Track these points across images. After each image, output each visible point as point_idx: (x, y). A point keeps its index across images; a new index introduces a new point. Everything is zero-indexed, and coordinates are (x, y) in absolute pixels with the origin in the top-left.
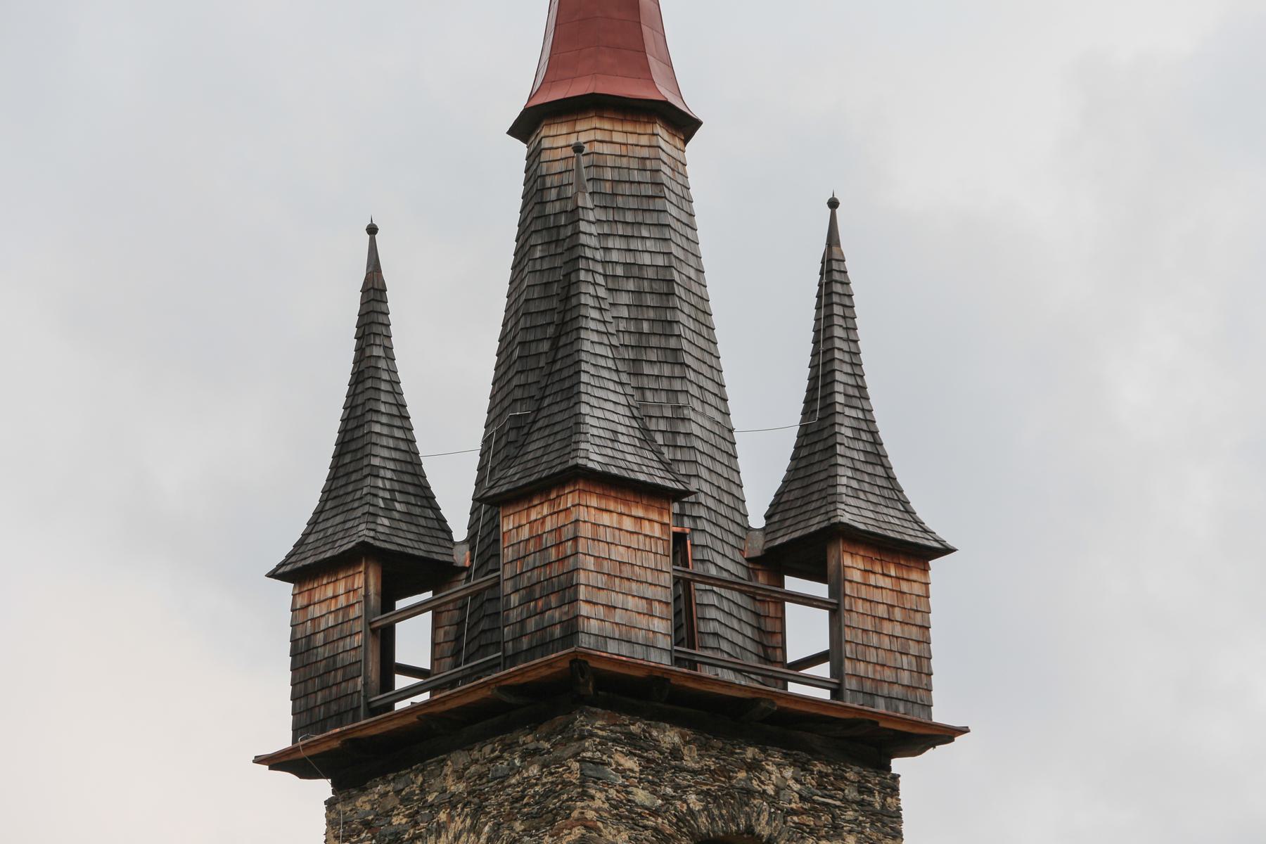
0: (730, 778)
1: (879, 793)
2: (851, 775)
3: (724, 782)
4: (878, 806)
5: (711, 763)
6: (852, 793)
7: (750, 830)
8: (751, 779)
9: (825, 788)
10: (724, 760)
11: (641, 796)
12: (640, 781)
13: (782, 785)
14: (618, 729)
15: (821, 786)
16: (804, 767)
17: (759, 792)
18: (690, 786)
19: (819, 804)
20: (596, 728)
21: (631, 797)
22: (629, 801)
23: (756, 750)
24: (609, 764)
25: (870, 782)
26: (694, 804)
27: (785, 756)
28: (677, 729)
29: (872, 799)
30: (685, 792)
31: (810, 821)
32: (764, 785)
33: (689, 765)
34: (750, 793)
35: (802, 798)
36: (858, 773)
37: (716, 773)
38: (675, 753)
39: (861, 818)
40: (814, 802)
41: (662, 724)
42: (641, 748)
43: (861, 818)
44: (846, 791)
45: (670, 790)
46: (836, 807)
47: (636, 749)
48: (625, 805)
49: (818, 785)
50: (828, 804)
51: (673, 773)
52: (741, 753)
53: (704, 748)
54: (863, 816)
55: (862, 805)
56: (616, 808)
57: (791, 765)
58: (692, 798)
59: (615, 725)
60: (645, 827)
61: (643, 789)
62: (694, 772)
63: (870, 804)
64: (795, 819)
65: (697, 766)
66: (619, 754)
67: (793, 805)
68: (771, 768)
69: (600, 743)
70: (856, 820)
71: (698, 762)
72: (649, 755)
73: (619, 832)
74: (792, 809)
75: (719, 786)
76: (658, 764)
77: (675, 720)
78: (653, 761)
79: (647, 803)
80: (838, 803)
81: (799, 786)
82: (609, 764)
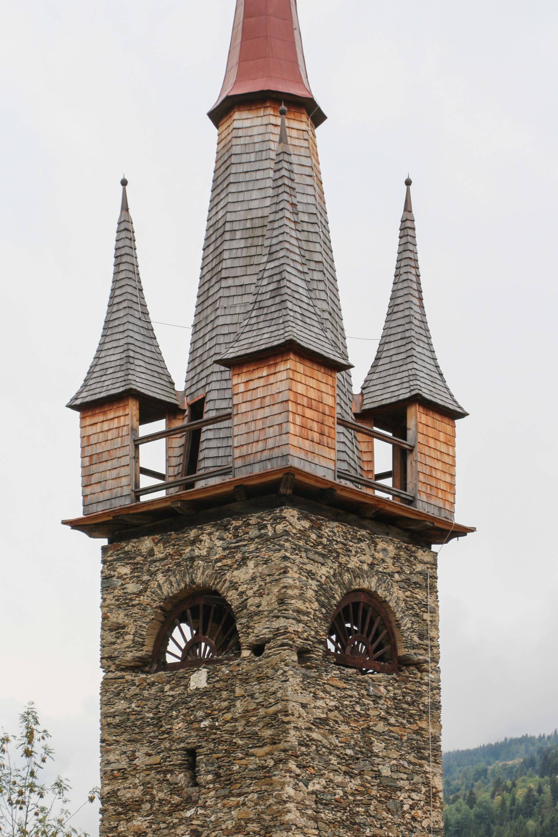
0: (181, 555)
1: (272, 524)
2: (253, 521)
3: (178, 559)
4: (270, 534)
5: (170, 550)
6: (253, 532)
7: (193, 582)
8: (194, 550)
9: (238, 536)
10: (178, 545)
11: (132, 587)
12: (131, 578)
13: (211, 546)
14: (120, 552)
15: (236, 536)
16: (226, 528)
17: (198, 556)
18: (158, 570)
19: (234, 548)
20: (108, 557)
21: (125, 591)
22: (125, 593)
23: (196, 530)
24: (114, 576)
25: (265, 520)
26: (161, 579)
27: (214, 526)
28: (151, 538)
29: (266, 531)
30: (155, 575)
31: (229, 562)
32: (201, 550)
33: (158, 556)
34: (192, 559)
35: (224, 549)
36: (258, 518)
37: (173, 555)
38: (151, 553)
39: (259, 547)
40: (231, 548)
41: (142, 538)
42: (131, 558)
43: (259, 547)
44: (250, 533)
45: (147, 577)
46: (245, 545)
47: (129, 560)
48: (123, 597)
49: (234, 536)
50: (239, 546)
51: (149, 565)
52: (187, 536)
53: (165, 543)
54: (260, 544)
55: (262, 537)
56: (118, 600)
57: (218, 530)
58: (160, 577)
59: (118, 550)
60: (133, 606)
61: (133, 582)
62: (162, 559)
63: (266, 534)
64: (219, 564)
65: (161, 556)
66: (120, 567)
67: (217, 556)
68: (205, 537)
69: (109, 565)
70: (257, 549)
71: (163, 553)
72: (136, 561)
73: (119, 614)
74: (217, 559)
75: (175, 562)
76: (141, 564)
77: (149, 532)
78: (138, 563)
79: (135, 590)
80: (246, 543)
81: (221, 542)
82: (114, 576)
